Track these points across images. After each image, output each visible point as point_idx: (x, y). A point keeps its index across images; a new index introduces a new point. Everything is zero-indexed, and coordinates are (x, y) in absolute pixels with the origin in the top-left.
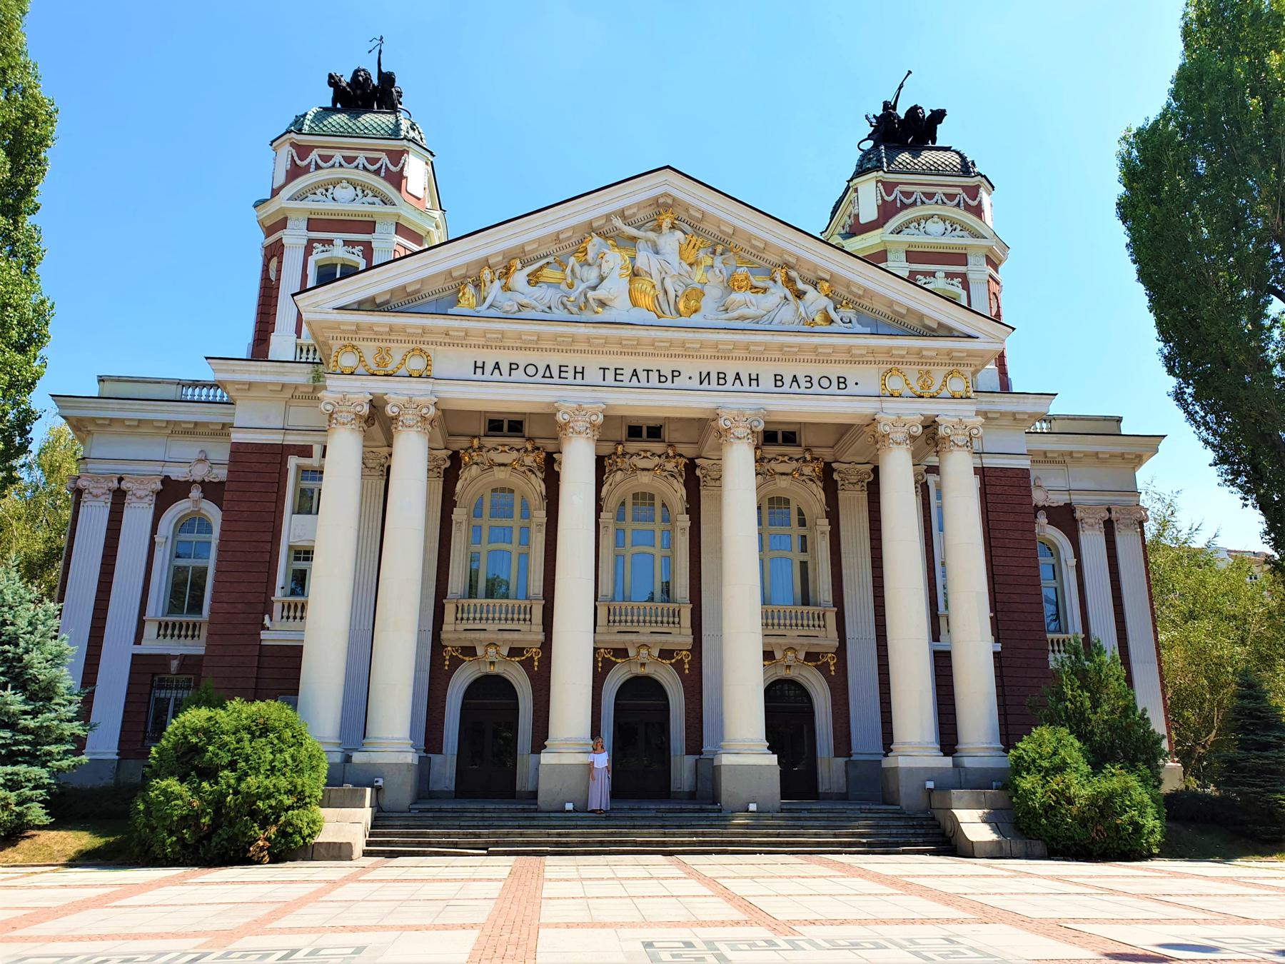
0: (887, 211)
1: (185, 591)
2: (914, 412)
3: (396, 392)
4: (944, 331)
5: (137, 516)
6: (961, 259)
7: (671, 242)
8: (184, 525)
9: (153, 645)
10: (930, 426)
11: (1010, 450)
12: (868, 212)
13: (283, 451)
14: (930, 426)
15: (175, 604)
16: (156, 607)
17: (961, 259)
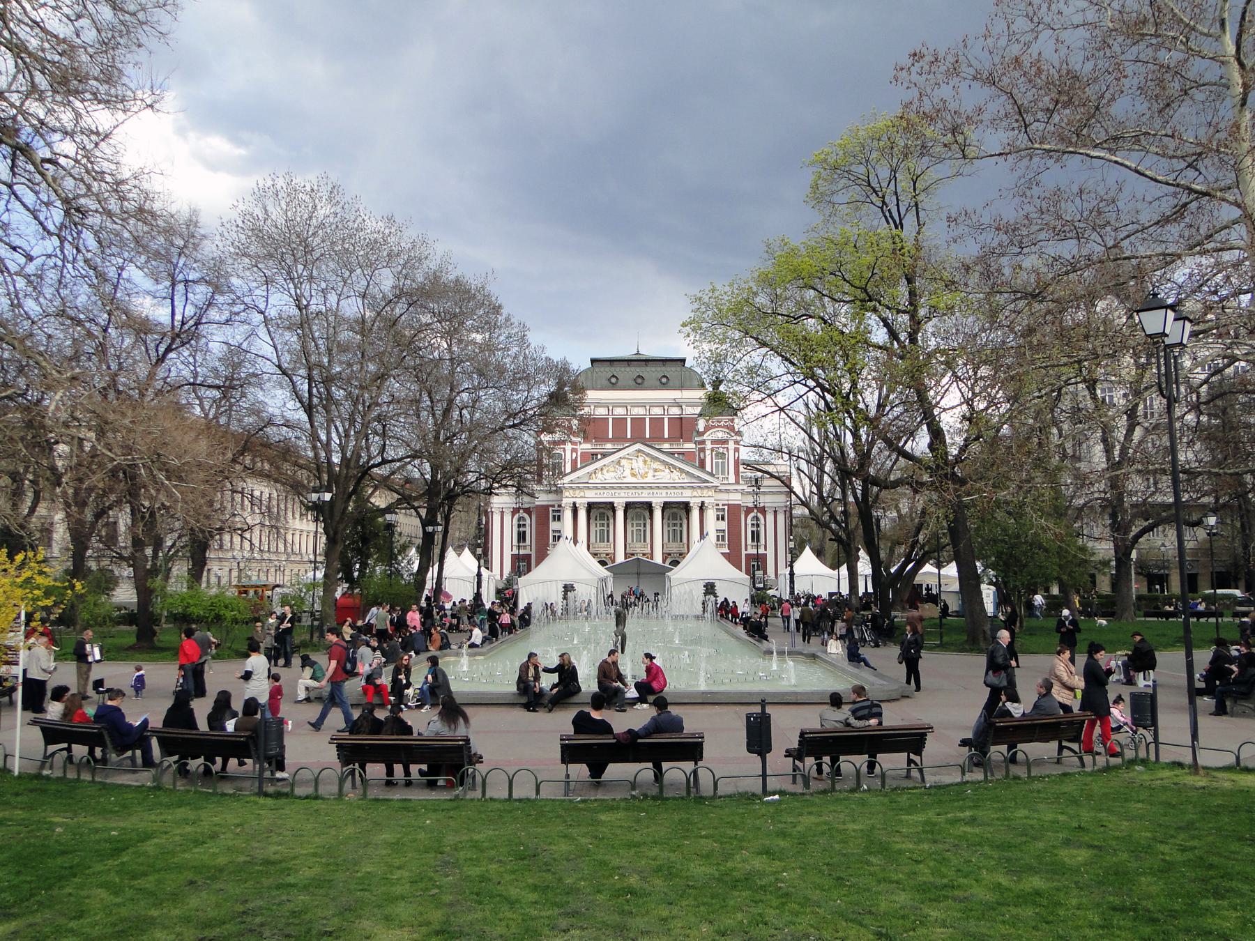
0: (707, 428)
1: (522, 537)
2: (700, 500)
3: (578, 501)
4: (707, 482)
5: (507, 518)
6: (726, 442)
7: (641, 459)
8: (519, 520)
9: (515, 552)
10: (703, 503)
11: (736, 498)
12: (701, 429)
13: (548, 506)
14: (703, 503)
15: (519, 541)
16: (515, 542)
17: (726, 442)
